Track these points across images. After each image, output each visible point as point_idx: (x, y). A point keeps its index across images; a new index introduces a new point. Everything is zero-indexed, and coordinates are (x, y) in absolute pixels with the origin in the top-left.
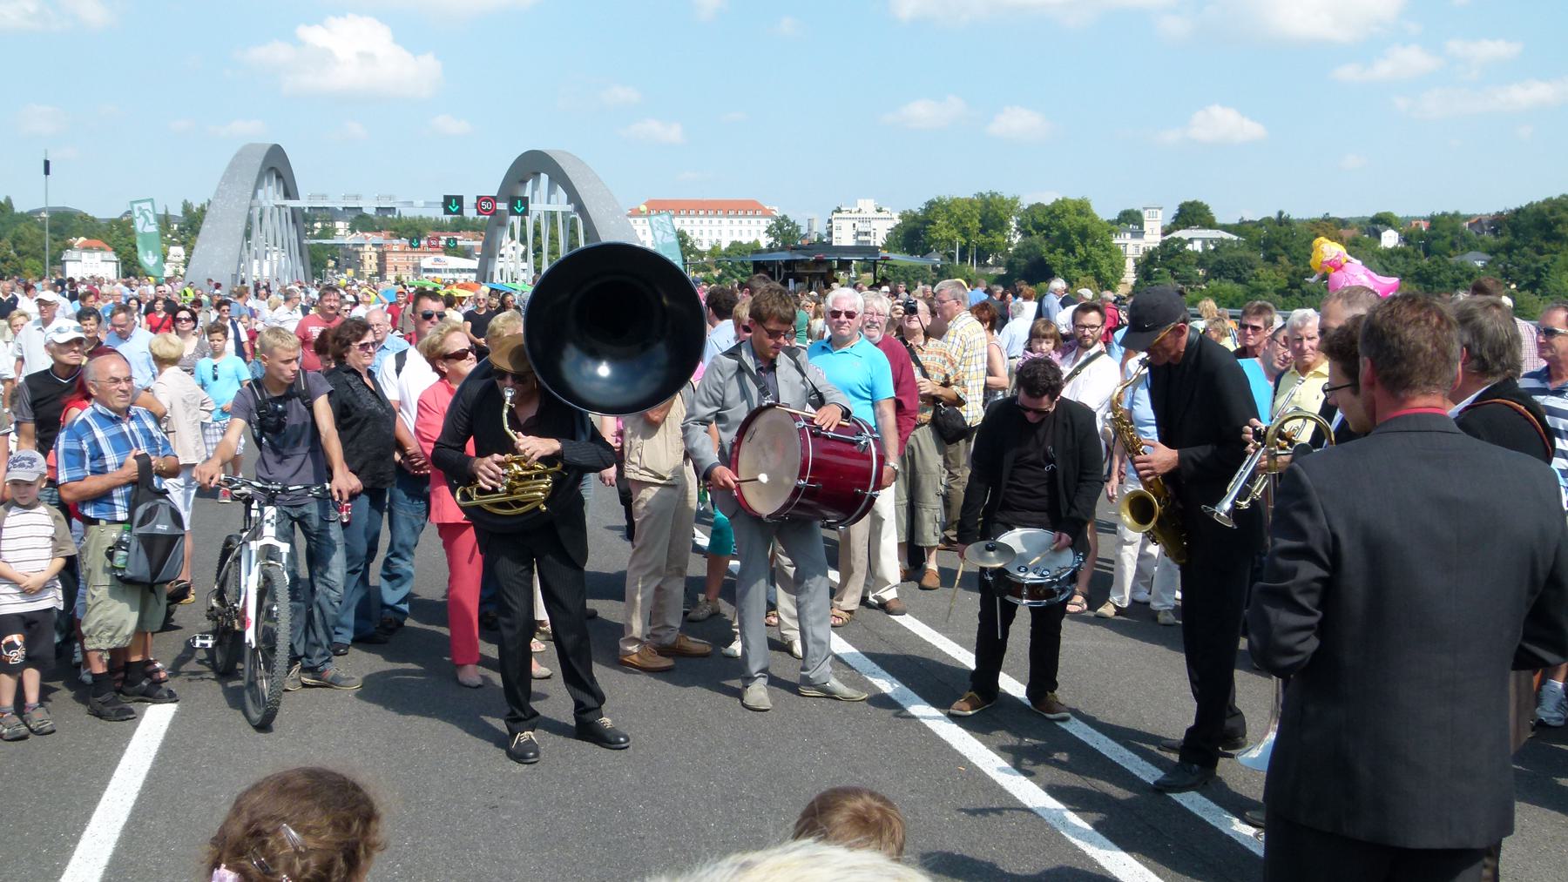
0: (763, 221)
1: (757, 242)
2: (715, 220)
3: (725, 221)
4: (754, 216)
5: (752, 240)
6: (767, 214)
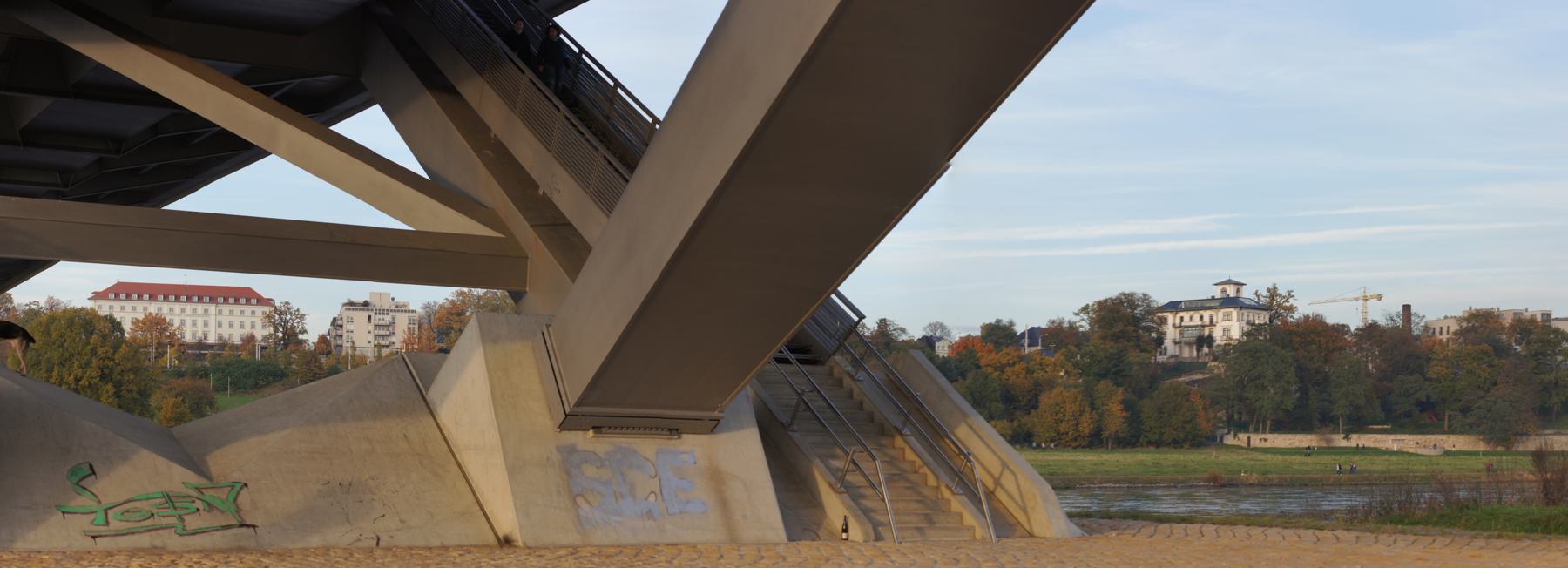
1: (251, 338)
3: (212, 308)
4: (248, 302)
5: (247, 331)
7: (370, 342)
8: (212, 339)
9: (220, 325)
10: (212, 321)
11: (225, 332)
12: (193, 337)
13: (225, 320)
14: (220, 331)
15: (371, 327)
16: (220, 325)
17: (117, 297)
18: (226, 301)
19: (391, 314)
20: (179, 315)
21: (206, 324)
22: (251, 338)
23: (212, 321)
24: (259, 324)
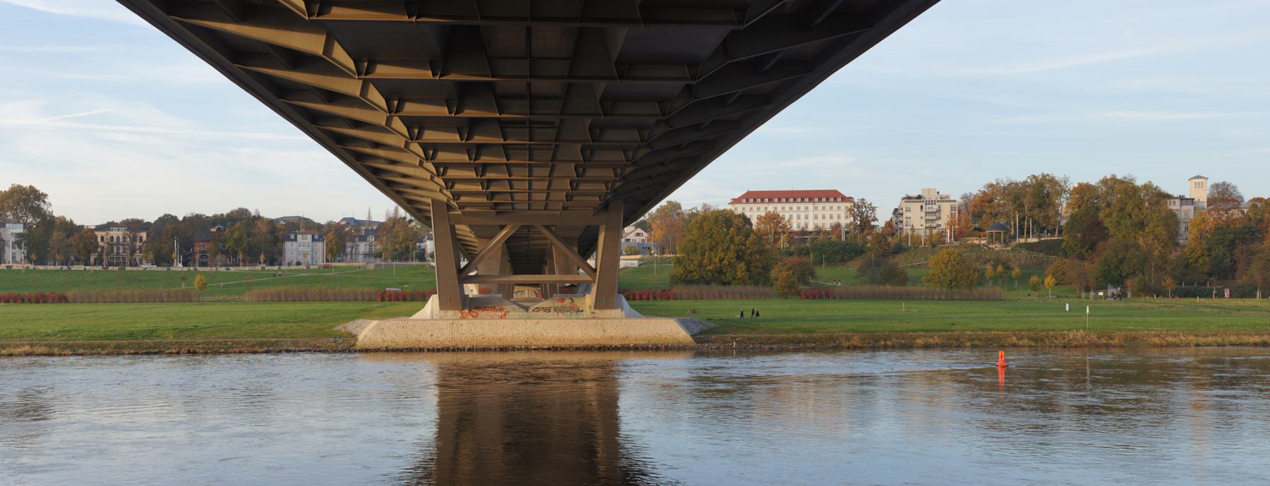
0: (844, 205)
3: (811, 206)
4: (835, 200)
5: (835, 221)
6: (844, 199)
7: (922, 225)
8: (811, 228)
9: (816, 217)
11: (820, 222)
12: (798, 227)
13: (820, 214)
14: (816, 221)
15: (923, 214)
16: (816, 217)
17: (747, 201)
18: (820, 200)
19: (938, 204)
20: (788, 212)
21: (806, 217)
22: (838, 226)
24: (843, 215)
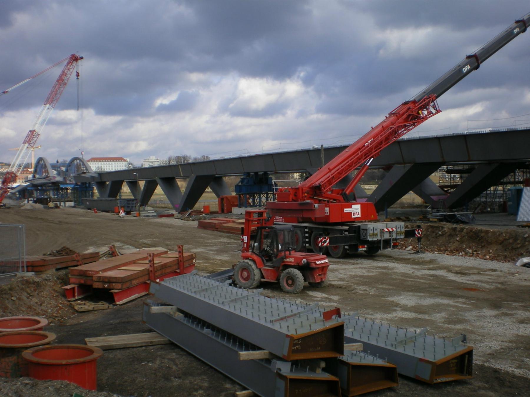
0: (124, 163)
2: (110, 163)
3: (113, 163)
4: (121, 161)
10: (113, 166)
12: (109, 170)
13: (116, 165)
16: (115, 166)
17: (92, 162)
21: (112, 166)
23: (113, 166)
